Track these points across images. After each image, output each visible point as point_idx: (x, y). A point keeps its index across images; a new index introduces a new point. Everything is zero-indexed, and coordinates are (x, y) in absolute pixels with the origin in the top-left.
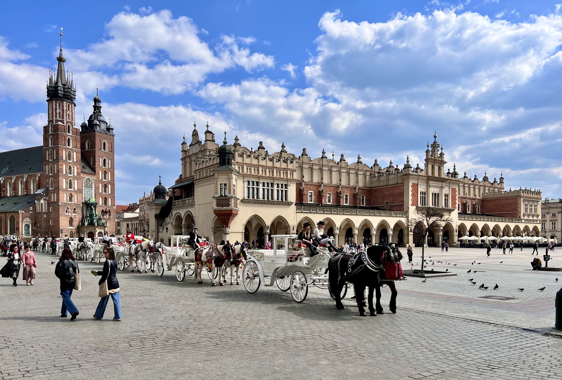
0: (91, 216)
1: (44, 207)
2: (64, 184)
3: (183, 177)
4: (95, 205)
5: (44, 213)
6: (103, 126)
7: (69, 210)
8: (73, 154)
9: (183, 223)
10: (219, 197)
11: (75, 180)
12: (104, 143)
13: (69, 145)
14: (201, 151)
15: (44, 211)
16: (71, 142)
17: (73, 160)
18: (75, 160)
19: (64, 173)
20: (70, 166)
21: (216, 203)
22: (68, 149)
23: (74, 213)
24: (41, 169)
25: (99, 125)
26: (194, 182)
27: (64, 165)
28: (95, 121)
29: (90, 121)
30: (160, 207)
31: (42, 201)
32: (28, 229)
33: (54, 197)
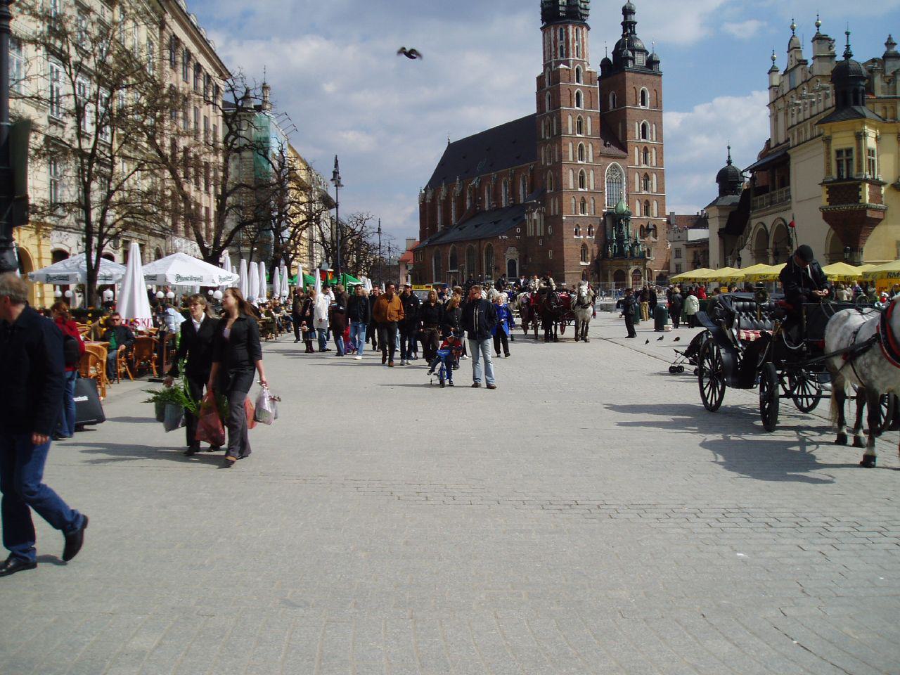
0: (620, 239)
2: (570, 180)
3: (772, 145)
4: (626, 216)
5: (540, 237)
6: (640, 60)
8: (586, 121)
9: (771, 245)
10: (834, 181)
12: (643, 93)
13: (578, 105)
14: (805, 82)
15: (538, 234)
17: (586, 134)
18: (589, 133)
20: (581, 146)
21: (827, 196)
23: (589, 235)
24: (534, 156)
25: (631, 59)
26: (789, 152)
27: (570, 144)
29: (617, 52)
30: (727, 213)
31: (535, 216)
33: (554, 206)
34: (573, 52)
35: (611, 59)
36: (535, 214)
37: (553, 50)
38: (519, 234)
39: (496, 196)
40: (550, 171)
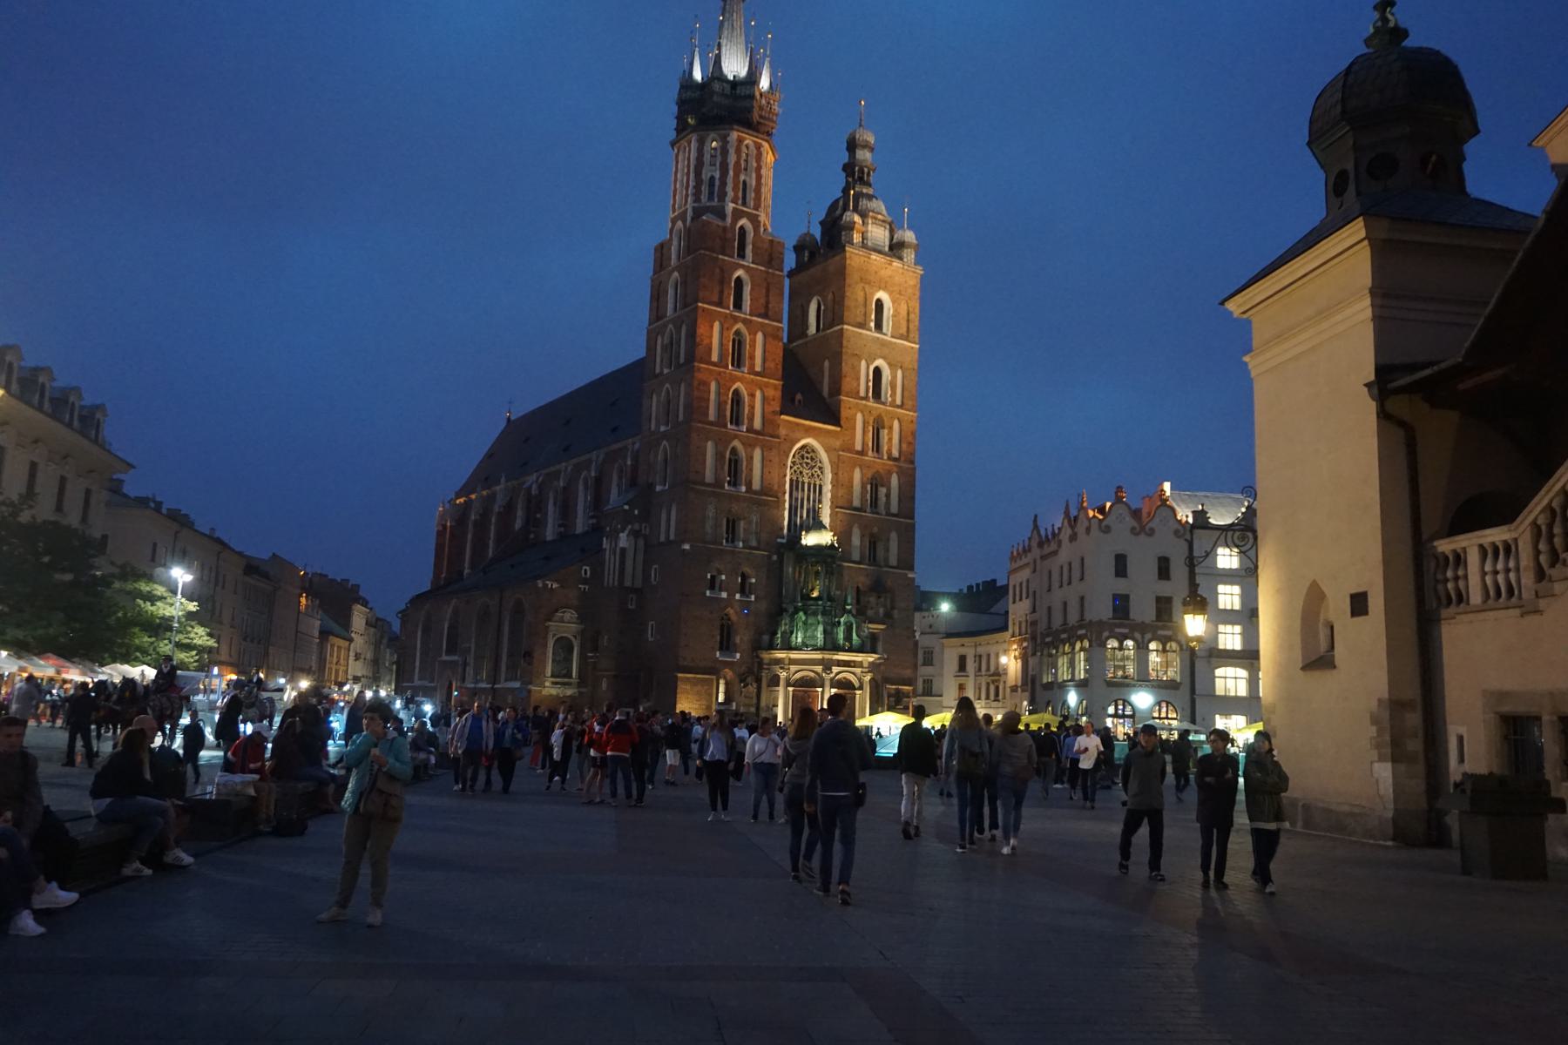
7: (723, 577)
8: (753, 342)
12: (879, 304)
13: (738, 305)
15: (628, 583)
16: (747, 290)
19: (712, 416)
22: (736, 320)
28: (848, 213)
31: (624, 540)
32: (569, 660)
33: (668, 520)
34: (735, 189)
35: (819, 240)
36: (623, 536)
37: (692, 184)
39: (566, 511)
40: (665, 442)
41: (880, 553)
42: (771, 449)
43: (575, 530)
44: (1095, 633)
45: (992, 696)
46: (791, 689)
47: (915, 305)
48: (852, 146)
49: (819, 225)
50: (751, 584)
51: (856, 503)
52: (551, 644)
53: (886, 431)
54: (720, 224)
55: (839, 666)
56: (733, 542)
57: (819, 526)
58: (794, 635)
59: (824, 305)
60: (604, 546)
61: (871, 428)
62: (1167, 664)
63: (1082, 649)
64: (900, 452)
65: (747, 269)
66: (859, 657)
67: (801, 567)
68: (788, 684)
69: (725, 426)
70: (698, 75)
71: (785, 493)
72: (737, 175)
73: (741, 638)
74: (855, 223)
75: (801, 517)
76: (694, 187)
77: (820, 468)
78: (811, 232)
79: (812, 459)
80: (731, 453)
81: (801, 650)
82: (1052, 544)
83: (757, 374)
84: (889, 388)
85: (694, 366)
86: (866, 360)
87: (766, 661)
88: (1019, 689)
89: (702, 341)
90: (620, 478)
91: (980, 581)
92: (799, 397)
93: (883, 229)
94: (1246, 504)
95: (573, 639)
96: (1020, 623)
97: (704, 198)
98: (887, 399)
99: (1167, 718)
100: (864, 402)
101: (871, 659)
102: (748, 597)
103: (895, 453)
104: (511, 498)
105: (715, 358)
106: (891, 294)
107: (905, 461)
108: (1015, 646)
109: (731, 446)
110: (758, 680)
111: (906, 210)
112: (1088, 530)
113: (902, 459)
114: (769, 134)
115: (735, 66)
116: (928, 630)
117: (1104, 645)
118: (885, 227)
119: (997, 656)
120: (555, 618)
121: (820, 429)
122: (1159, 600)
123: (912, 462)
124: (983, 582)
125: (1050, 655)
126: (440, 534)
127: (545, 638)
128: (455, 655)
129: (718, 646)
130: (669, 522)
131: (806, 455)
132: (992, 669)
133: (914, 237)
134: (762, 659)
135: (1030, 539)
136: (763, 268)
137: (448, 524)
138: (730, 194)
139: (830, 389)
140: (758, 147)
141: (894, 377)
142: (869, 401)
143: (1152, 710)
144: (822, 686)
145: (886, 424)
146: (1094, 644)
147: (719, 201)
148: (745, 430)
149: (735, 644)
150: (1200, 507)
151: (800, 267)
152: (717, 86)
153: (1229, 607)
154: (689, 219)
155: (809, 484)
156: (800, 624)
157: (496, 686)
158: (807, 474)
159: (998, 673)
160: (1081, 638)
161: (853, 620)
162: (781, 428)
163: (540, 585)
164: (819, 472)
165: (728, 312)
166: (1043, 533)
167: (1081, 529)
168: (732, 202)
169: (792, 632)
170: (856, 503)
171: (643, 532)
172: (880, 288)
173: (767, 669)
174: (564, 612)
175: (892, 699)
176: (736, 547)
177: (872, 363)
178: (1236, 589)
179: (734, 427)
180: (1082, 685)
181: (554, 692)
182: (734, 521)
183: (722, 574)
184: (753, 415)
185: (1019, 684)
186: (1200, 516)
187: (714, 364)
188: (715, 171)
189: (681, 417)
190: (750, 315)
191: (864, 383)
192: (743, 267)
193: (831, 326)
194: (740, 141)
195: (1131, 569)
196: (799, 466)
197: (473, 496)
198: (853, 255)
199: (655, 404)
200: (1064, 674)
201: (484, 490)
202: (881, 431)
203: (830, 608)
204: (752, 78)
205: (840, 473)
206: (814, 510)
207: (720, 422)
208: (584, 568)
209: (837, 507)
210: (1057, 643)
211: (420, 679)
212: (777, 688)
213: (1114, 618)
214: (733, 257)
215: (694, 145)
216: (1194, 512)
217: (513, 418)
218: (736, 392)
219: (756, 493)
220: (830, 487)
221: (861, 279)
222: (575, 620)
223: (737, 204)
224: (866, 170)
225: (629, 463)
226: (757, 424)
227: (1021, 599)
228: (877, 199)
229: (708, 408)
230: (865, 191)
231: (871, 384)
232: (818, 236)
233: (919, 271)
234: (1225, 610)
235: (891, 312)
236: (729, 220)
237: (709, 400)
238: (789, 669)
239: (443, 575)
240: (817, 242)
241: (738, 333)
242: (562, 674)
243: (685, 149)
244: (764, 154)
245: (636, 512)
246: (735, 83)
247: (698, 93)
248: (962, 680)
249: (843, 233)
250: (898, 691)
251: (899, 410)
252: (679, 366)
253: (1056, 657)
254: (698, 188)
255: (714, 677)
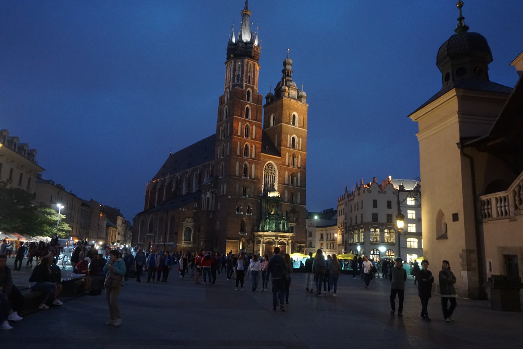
1: (210, 202)
7: (242, 207)
8: (252, 129)
11: (252, 164)
12: (294, 116)
13: (247, 116)
15: (210, 209)
19: (238, 153)
28: (284, 86)
31: (208, 195)
34: (246, 78)
36: (208, 193)
37: (232, 76)
38: (195, 209)
39: (189, 185)
40: (222, 162)
41: (294, 199)
42: (258, 164)
43: (192, 191)
44: (366, 227)
45: (332, 248)
46: (264, 245)
47: (306, 116)
48: (285, 64)
49: (274, 90)
50: (251, 209)
51: (286, 183)
52: (184, 229)
53: (296, 158)
54: (241, 89)
55: (280, 237)
56: (245, 195)
57: (274, 190)
58: (265, 227)
59: (276, 117)
60: (202, 197)
61: (291, 158)
62: (391, 237)
63: (362, 232)
64: (301, 166)
65: (250, 105)
66: (287, 234)
67: (268, 204)
68: (263, 243)
69: (243, 157)
70: (234, 41)
71: (262, 179)
72: (247, 74)
73: (248, 228)
74: (286, 89)
75: (268, 187)
76: (233, 78)
77: (274, 171)
78: (271, 92)
79: (272, 168)
80: (244, 166)
81: (268, 232)
82: (352, 196)
83: (254, 139)
84: (297, 144)
85: (232, 137)
86: (290, 135)
87: (256, 236)
88: (341, 245)
89: (235, 128)
90: (207, 174)
91: (328, 209)
92: (267, 147)
93: (295, 91)
94: (417, 183)
95: (191, 228)
96: (341, 223)
97: (236, 81)
98: (297, 148)
99: (391, 255)
100: (289, 149)
101: (291, 235)
102: (250, 214)
103: (299, 166)
104: (171, 181)
105: (239, 134)
106: (298, 113)
107: (303, 169)
108: (340, 231)
109: (244, 163)
110: (253, 242)
111: (303, 85)
112: (364, 192)
113: (302, 168)
114: (257, 60)
115: (246, 38)
116: (310, 225)
117: (369, 230)
118: (296, 91)
119: (334, 234)
120: (185, 221)
121: (274, 158)
122: (388, 215)
123: (305, 169)
124: (329, 209)
125: (351, 234)
126: (147, 193)
127: (182, 228)
128: (152, 233)
129: (240, 231)
130: (224, 189)
131: (270, 166)
132: (332, 238)
133: (305, 94)
134: (255, 235)
135: (344, 195)
136: (255, 104)
137: (150, 189)
138: (244, 78)
139: (278, 145)
140: (254, 64)
141: (299, 140)
142: (290, 148)
143: (385, 252)
144: (275, 244)
145: (296, 156)
146: (366, 230)
147: (241, 82)
148: (249, 158)
149: (246, 230)
150: (401, 184)
151: (268, 104)
152: (240, 44)
153: (411, 218)
154: (231, 88)
155: (271, 176)
156: (268, 223)
157: (165, 244)
158: (270, 173)
159: (334, 240)
160: (362, 228)
161: (285, 222)
162: (261, 157)
163: (181, 210)
164: (274, 172)
165: (244, 119)
166: (349, 193)
167: (361, 191)
168: (245, 82)
169: (265, 226)
170: (286, 183)
171: (215, 192)
172: (294, 111)
173: (256, 238)
174: (188, 219)
175: (299, 248)
176: (246, 197)
177: (292, 136)
178: (414, 212)
179: (245, 157)
180: (362, 244)
181: (185, 246)
182: (245, 188)
183: (241, 206)
184: (252, 153)
185: (341, 244)
186: (401, 187)
187: (239, 136)
188: (240, 72)
189: (228, 154)
190: (251, 120)
191: (289, 143)
192: (249, 104)
193: (279, 123)
194: (248, 62)
195: (378, 205)
196: (267, 170)
197: (158, 180)
198: (285, 100)
199: (219, 149)
200: (356, 240)
201: (162, 178)
202: (295, 158)
203: (278, 218)
204: (252, 42)
205: (281, 172)
206: (272, 185)
207: (241, 155)
208: (195, 204)
209: (280, 184)
210: (354, 229)
211: (140, 241)
212: (260, 245)
213: (373, 221)
214: (245, 101)
215: (233, 64)
216: (399, 186)
217: (172, 154)
218: (246, 145)
219: (252, 179)
220: (277, 177)
221: (288, 108)
222: (192, 222)
223: (247, 83)
224: (290, 72)
225: (210, 169)
226: (253, 156)
227: (341, 215)
228: (293, 82)
229: (237, 151)
230: (289, 79)
231: (291, 143)
232: (274, 94)
233: (307, 105)
234: (410, 219)
235: (298, 119)
236: (244, 89)
237: (237, 148)
238: (264, 238)
239: (148, 206)
240: (273, 96)
241: (247, 126)
242: (187, 239)
243: (230, 64)
244: (256, 67)
245: (213, 185)
246: (246, 43)
247: (234, 46)
248: (322, 242)
249: (282, 93)
250: (300, 246)
251: (301, 152)
252: (227, 137)
253: (354, 234)
254: (234, 78)
255: (239, 241)
